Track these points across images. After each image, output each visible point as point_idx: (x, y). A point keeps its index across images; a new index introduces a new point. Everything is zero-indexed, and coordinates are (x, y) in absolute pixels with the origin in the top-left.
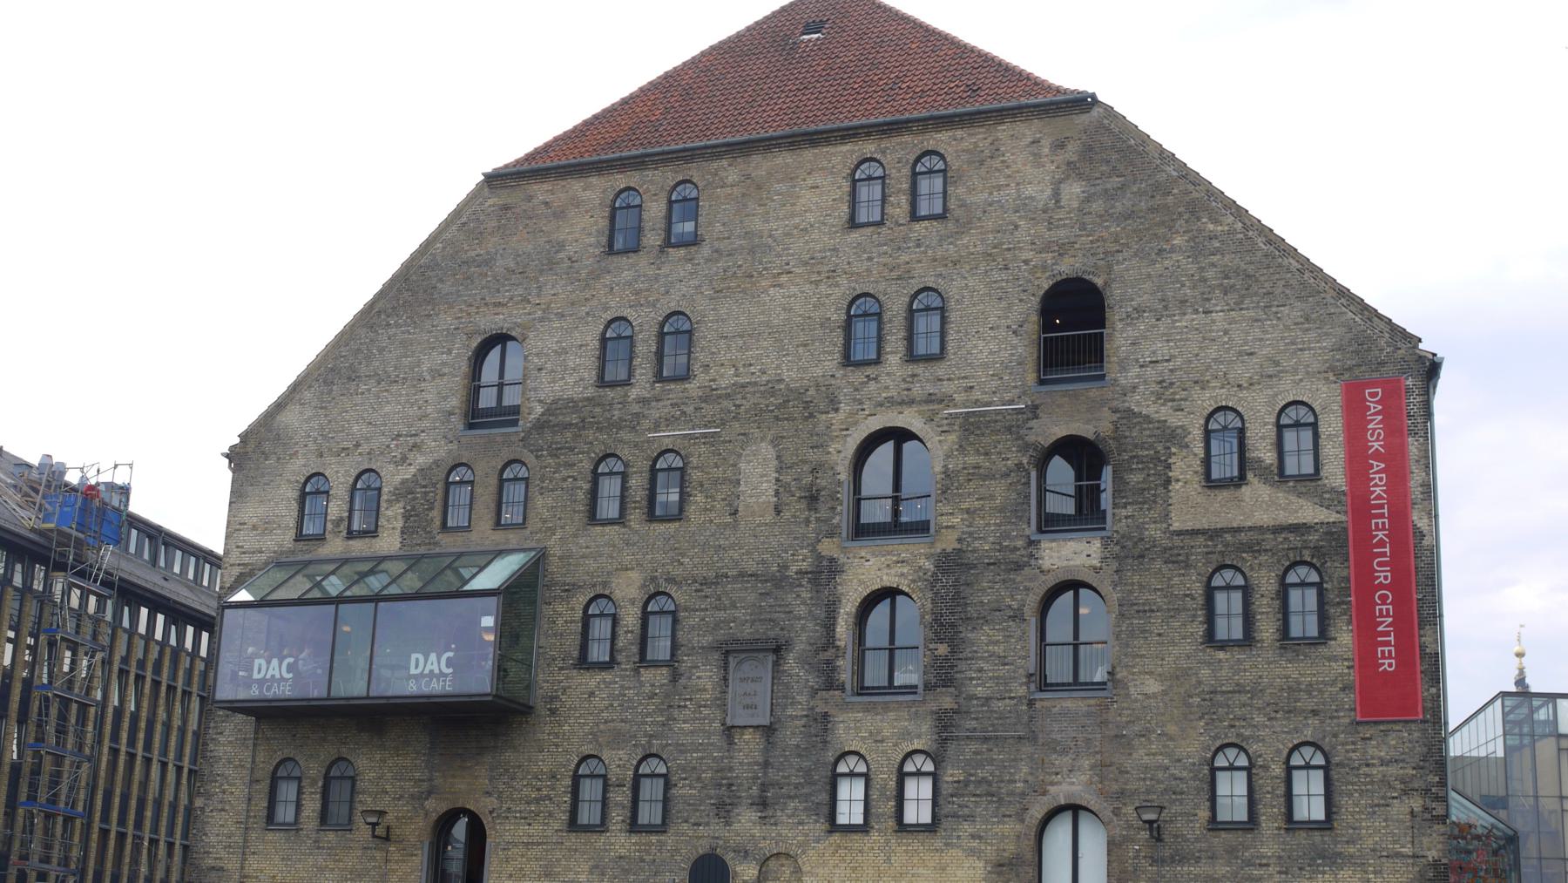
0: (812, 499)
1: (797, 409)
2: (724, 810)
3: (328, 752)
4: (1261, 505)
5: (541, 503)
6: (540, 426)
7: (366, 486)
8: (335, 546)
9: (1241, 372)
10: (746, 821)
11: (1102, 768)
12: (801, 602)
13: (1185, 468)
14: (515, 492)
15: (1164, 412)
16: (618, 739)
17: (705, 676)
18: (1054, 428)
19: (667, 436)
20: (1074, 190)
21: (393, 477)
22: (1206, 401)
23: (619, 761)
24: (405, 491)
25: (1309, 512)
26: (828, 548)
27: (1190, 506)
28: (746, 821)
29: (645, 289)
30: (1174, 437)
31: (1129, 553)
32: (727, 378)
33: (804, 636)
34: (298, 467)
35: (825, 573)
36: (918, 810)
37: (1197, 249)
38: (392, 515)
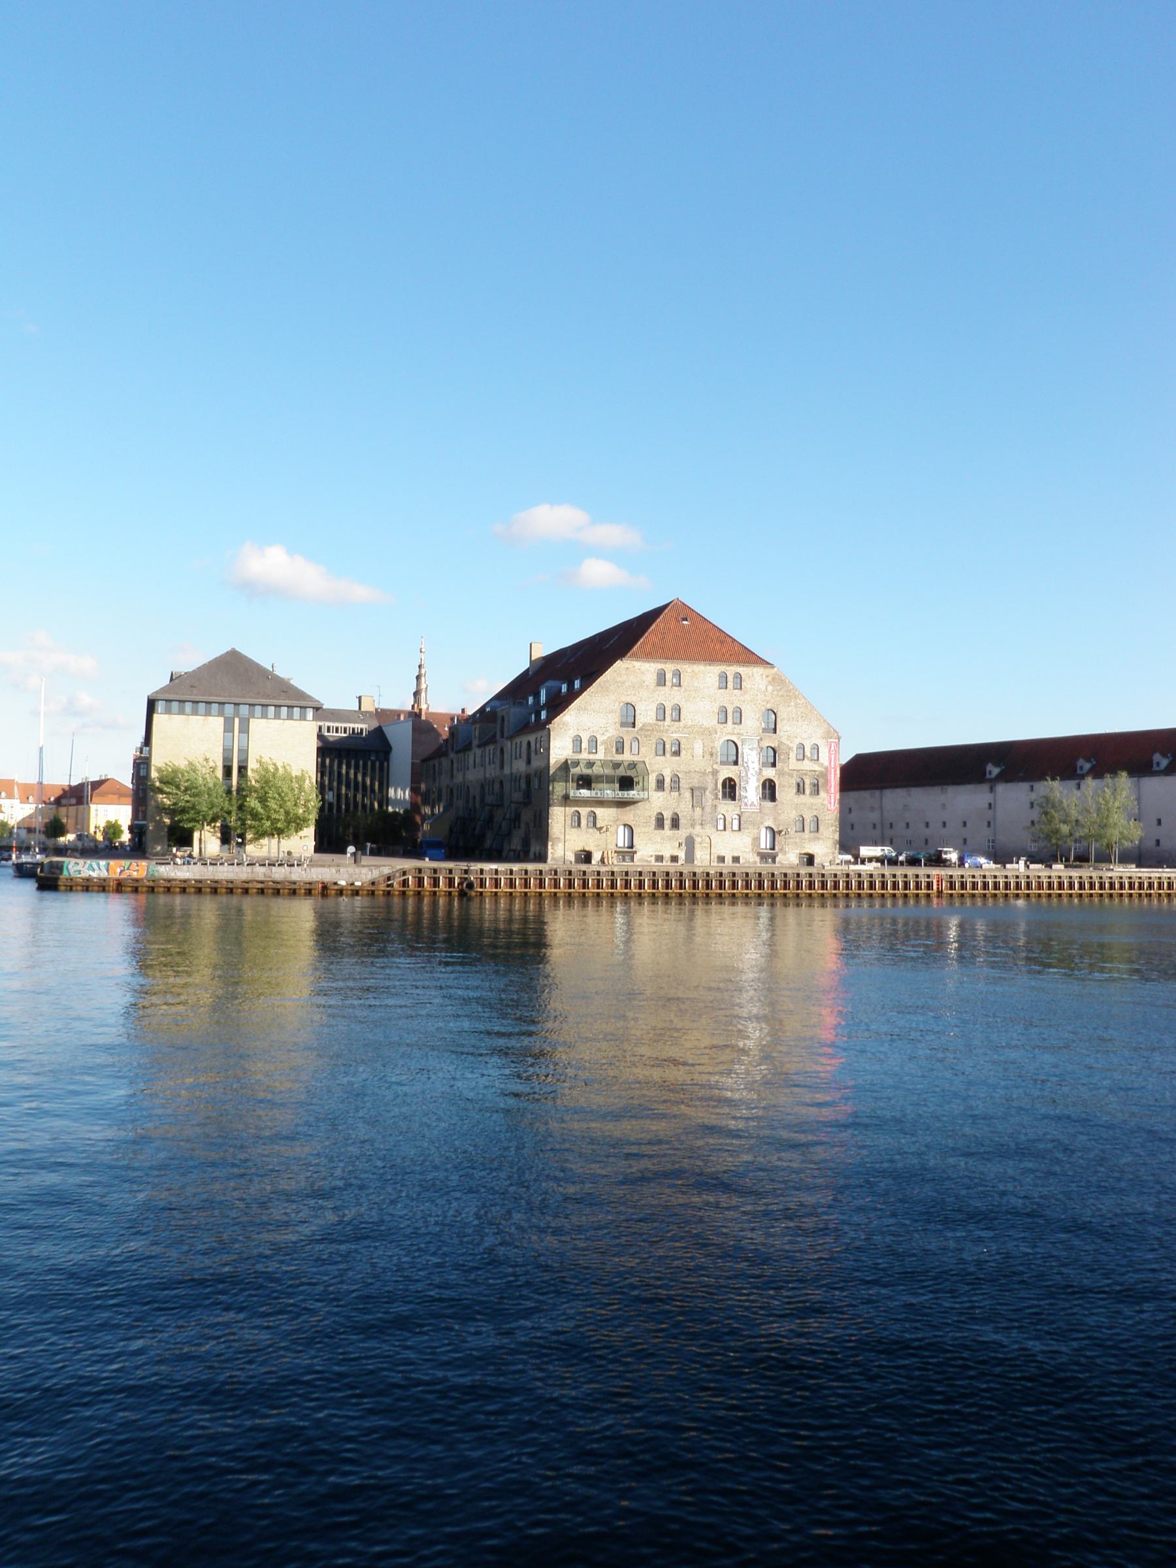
0: (712, 755)
1: (709, 733)
2: (693, 826)
3: (589, 809)
4: (807, 765)
5: (642, 749)
6: (641, 729)
7: (594, 741)
8: (584, 756)
9: (804, 736)
10: (698, 828)
11: (775, 819)
12: (710, 779)
13: (793, 756)
14: (635, 745)
15: (788, 743)
16: (666, 809)
17: (688, 795)
18: (765, 744)
19: (675, 736)
20: (770, 688)
21: (600, 739)
22: (797, 741)
23: (668, 816)
24: (604, 743)
25: (817, 768)
26: (715, 766)
27: (793, 764)
28: (698, 828)
29: (669, 696)
30: (790, 748)
31: (781, 774)
32: (690, 723)
33: (710, 786)
34: (572, 733)
35: (715, 773)
36: (736, 827)
37: (796, 705)
38: (601, 748)
